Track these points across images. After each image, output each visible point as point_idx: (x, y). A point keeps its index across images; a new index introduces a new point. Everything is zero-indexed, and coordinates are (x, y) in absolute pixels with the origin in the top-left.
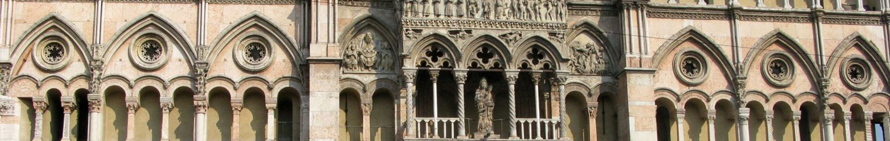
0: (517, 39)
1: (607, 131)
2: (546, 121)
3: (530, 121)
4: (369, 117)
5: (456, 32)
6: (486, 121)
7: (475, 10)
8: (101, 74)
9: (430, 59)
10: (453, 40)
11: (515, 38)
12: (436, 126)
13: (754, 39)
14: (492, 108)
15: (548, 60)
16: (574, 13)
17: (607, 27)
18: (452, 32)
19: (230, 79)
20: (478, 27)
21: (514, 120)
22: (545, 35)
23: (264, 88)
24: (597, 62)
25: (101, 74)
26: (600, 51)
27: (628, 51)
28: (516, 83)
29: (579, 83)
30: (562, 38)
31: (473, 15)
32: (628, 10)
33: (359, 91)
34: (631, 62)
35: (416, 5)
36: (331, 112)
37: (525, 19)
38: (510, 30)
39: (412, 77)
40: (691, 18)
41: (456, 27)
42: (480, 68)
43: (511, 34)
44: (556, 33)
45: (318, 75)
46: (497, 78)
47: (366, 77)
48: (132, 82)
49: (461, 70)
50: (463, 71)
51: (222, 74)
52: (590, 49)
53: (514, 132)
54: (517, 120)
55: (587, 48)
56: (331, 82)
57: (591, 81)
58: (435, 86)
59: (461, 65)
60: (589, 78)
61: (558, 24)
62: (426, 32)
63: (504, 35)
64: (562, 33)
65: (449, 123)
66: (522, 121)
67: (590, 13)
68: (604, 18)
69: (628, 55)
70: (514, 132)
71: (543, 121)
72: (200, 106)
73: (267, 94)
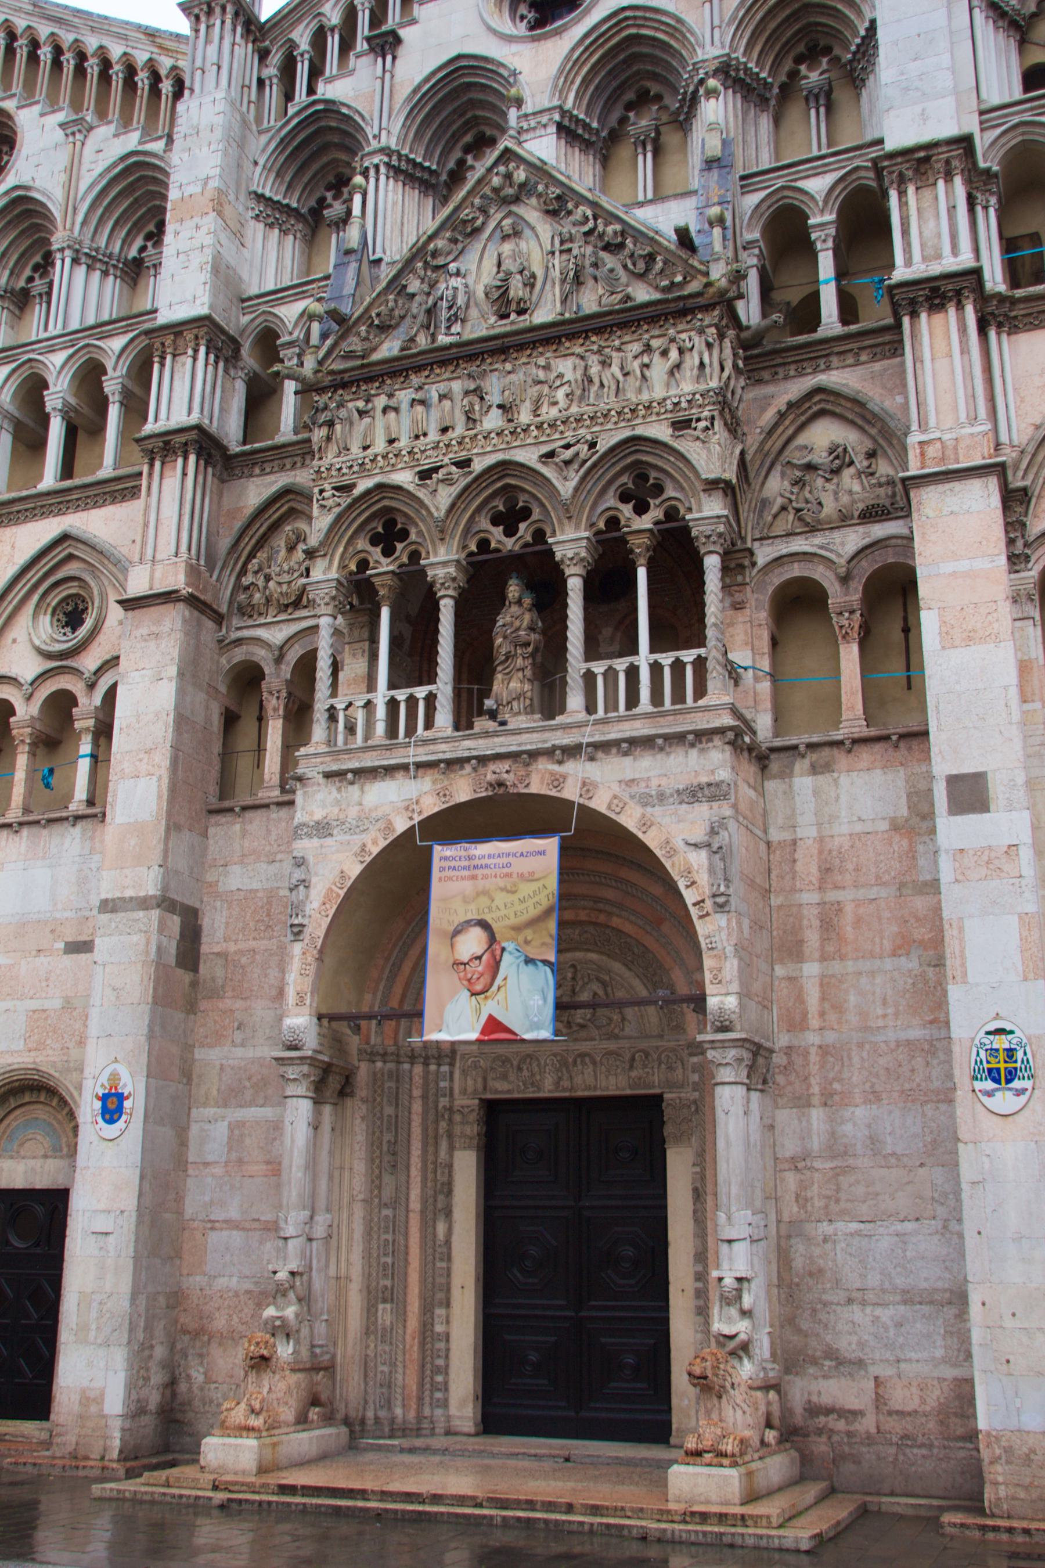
0: (582, 456)
3: (621, 665)
4: (281, 721)
5: (436, 470)
6: (514, 685)
7: (477, 408)
9: (379, 550)
10: (421, 494)
11: (577, 454)
12: (381, 712)
14: (530, 649)
15: (673, 494)
16: (792, 373)
17: (884, 387)
18: (425, 475)
19: (15, 679)
20: (489, 449)
22: (661, 431)
23: (76, 687)
24: (856, 488)
27: (914, 427)
28: (588, 572)
29: (805, 553)
30: (707, 428)
31: (475, 421)
32: (914, 315)
33: (263, 664)
34: (922, 454)
35: (338, 427)
37: (609, 401)
38: (569, 436)
39: (327, 599)
42: (497, 550)
43: (567, 447)
44: (691, 420)
45: (138, 633)
47: (281, 630)
50: (445, 564)
52: (837, 457)
53: (575, 700)
54: (584, 666)
55: (830, 454)
57: (843, 544)
59: (442, 550)
60: (837, 535)
61: (694, 394)
63: (551, 454)
64: (706, 414)
65: (412, 701)
66: (599, 668)
67: (835, 360)
68: (877, 366)
69: (914, 439)
71: (656, 662)
73: (82, 700)
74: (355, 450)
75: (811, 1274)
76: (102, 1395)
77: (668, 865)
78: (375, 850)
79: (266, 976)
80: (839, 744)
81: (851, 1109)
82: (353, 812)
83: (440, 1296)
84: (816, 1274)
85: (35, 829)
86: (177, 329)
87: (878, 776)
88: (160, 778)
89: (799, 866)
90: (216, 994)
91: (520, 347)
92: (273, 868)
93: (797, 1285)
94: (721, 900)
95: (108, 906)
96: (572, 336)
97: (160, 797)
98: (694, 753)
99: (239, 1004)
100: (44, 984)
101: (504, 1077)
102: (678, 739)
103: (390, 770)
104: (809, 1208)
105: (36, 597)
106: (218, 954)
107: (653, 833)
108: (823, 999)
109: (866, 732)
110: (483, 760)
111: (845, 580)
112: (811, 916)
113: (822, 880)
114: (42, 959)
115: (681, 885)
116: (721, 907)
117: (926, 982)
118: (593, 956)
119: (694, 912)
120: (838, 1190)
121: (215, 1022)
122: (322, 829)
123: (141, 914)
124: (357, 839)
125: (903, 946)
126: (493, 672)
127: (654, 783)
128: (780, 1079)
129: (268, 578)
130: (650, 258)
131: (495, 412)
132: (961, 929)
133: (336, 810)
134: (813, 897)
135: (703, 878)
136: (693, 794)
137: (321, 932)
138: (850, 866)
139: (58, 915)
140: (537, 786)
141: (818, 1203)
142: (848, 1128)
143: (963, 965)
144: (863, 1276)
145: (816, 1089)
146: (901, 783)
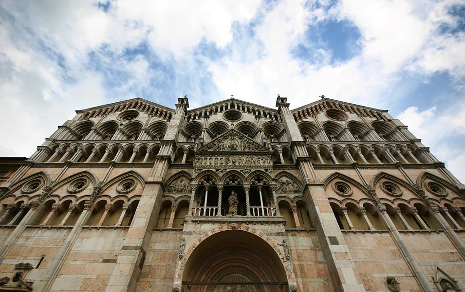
1: (305, 222)
2: (267, 208)
3: (258, 208)
8: (47, 194)
12: (205, 211)
13: (370, 176)
18: (218, 170)
19: (110, 196)
21: (248, 207)
22: (264, 171)
23: (125, 200)
24: (292, 187)
25: (47, 194)
26: (293, 183)
36: (150, 205)
40: (335, 169)
41: (219, 168)
46: (240, 190)
48: (61, 197)
49: (220, 185)
50: (221, 185)
51: (106, 194)
53: (249, 213)
56: (154, 191)
58: (207, 192)
60: (290, 195)
62: (204, 170)
63: (242, 171)
65: (212, 210)
66: (254, 208)
69: (307, 179)
70: (249, 213)
72: (86, 206)
74: (203, 164)
77: (274, 249)
78: (203, 239)
79: (161, 272)
80: (297, 230)
82: (198, 230)
85: (104, 230)
86: (167, 142)
87: (305, 238)
88: (147, 218)
89: (292, 255)
90: (146, 276)
91: (236, 155)
92: (168, 245)
94: (288, 258)
95: (125, 248)
96: (246, 155)
97: (146, 222)
98: (277, 226)
99: (152, 280)
100: (93, 271)
102: (274, 222)
103: (208, 222)
105: (121, 181)
106: (148, 265)
107: (270, 241)
108: (304, 288)
109: (302, 229)
110: (231, 222)
111: (292, 202)
112: (297, 266)
113: (298, 259)
114: (95, 264)
115: (278, 254)
116: (288, 260)
117: (326, 285)
118: (240, 275)
119: (282, 260)
121: (144, 285)
122: (190, 233)
123: (135, 250)
124: (199, 237)
125: (319, 276)
126: (229, 207)
127: (269, 231)
129: (176, 185)
130: (258, 147)
131: (231, 163)
132: (341, 270)
133: (194, 229)
134: (297, 263)
135: (283, 253)
136: (278, 234)
137: (187, 258)
138: (304, 256)
139: (103, 252)
140: (242, 229)
143: (344, 279)
146: (310, 240)
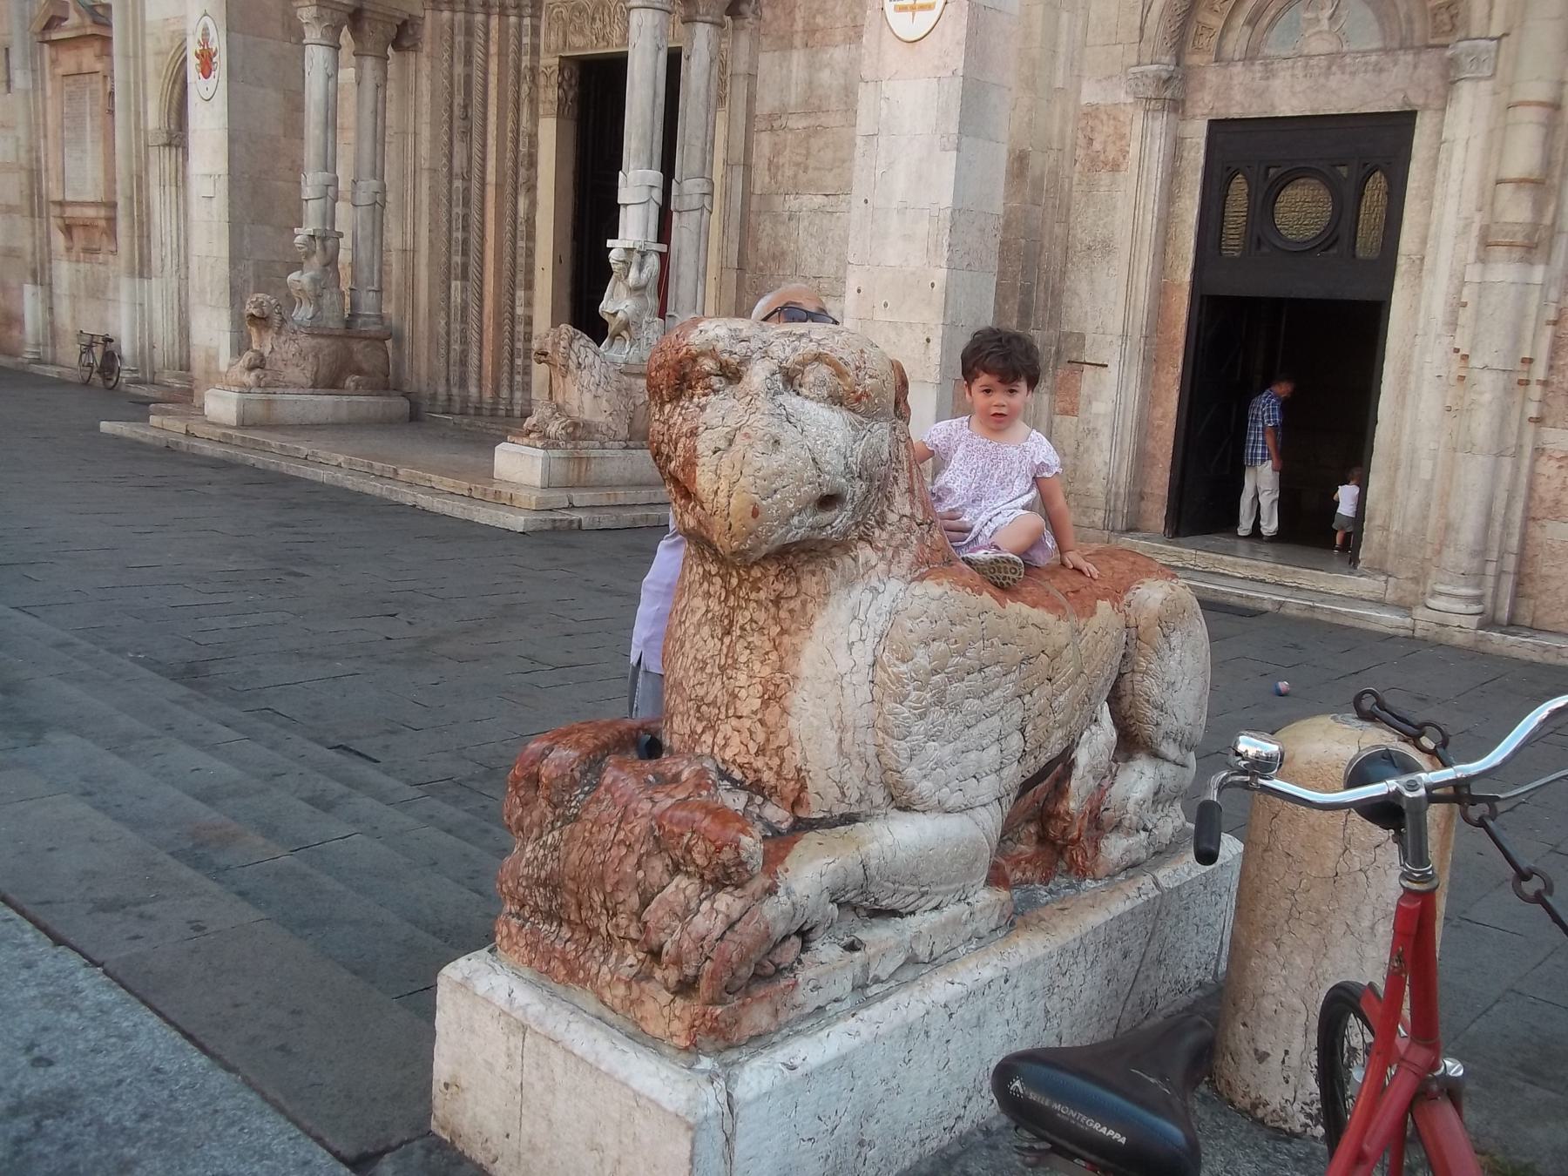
75: (774, 258)
76: (218, 354)
81: (831, 50)
83: (520, 277)
84: (779, 257)
93: (761, 270)
101: (581, 31)
104: (780, 178)
120: (808, 155)
128: (767, 13)
141: (789, 172)
142: (825, 75)
144: (821, 261)
145: (799, 25)
